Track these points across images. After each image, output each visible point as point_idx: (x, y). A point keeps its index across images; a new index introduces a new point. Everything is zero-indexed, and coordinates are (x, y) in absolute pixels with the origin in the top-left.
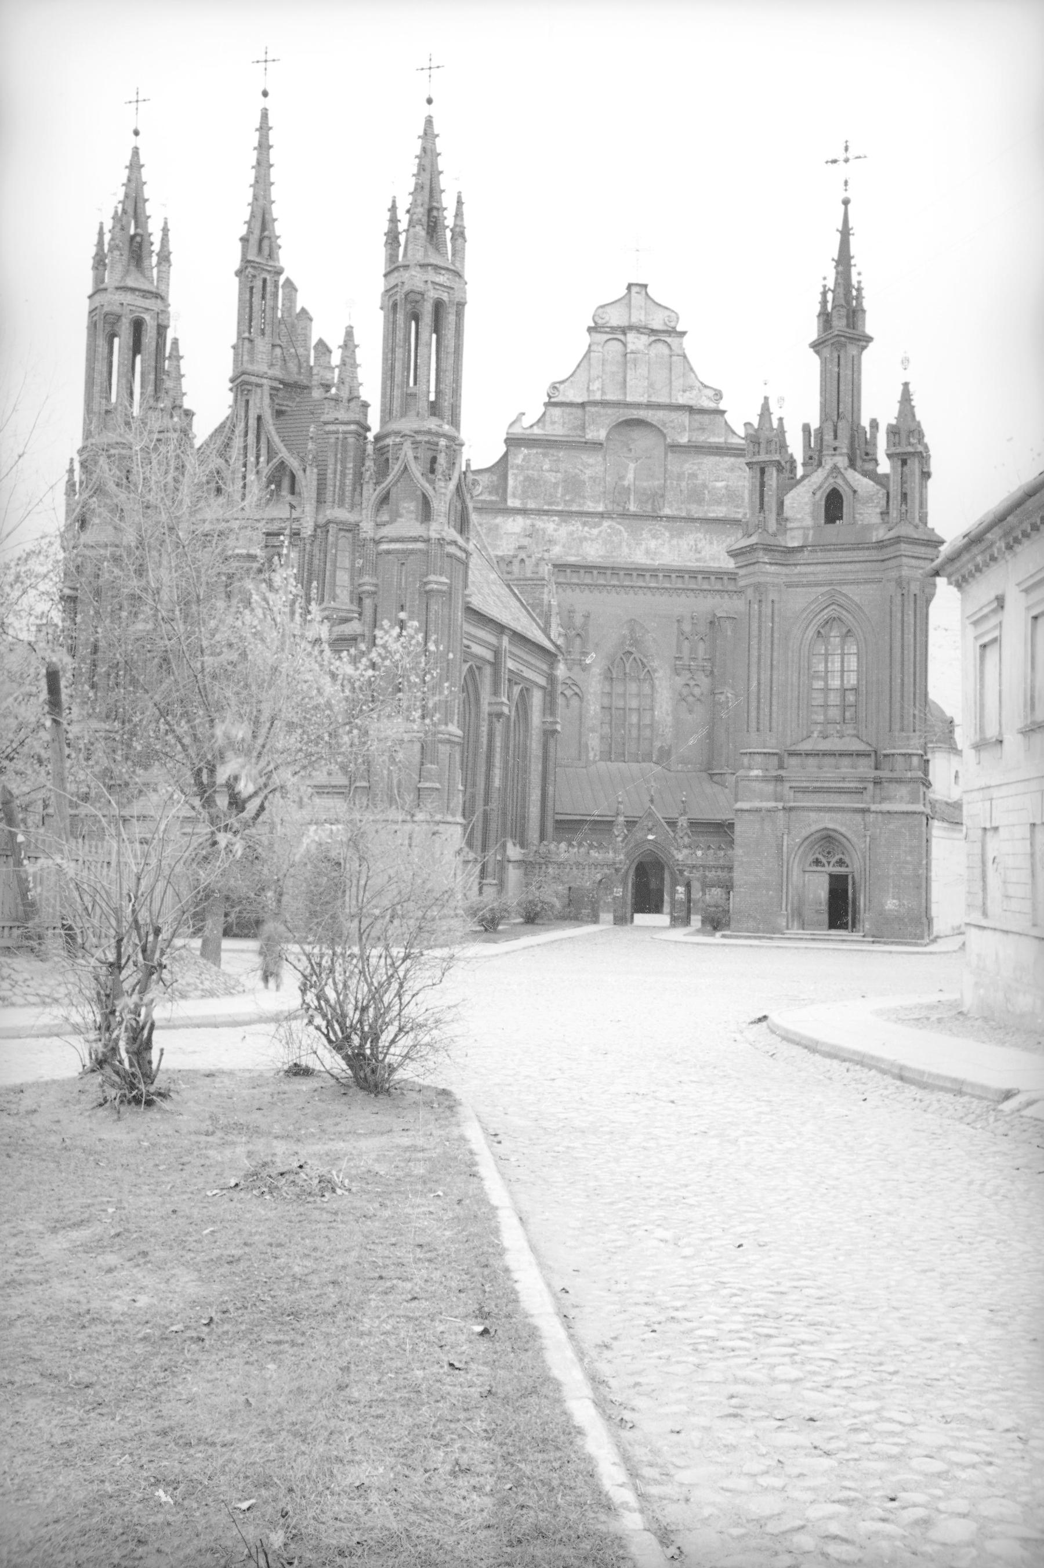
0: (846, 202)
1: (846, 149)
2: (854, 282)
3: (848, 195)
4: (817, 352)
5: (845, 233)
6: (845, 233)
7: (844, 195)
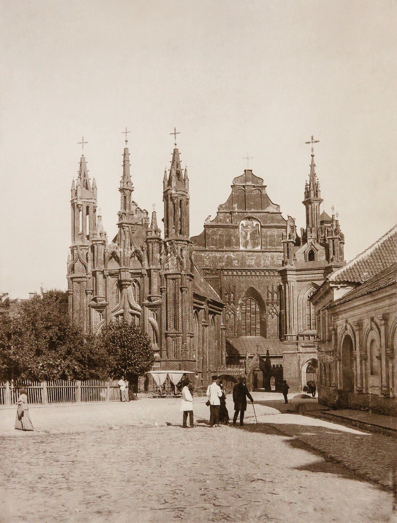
0: (313, 156)
1: (312, 139)
2: (317, 181)
3: (314, 153)
4: (304, 204)
5: (313, 166)
6: (313, 166)
7: (311, 153)
